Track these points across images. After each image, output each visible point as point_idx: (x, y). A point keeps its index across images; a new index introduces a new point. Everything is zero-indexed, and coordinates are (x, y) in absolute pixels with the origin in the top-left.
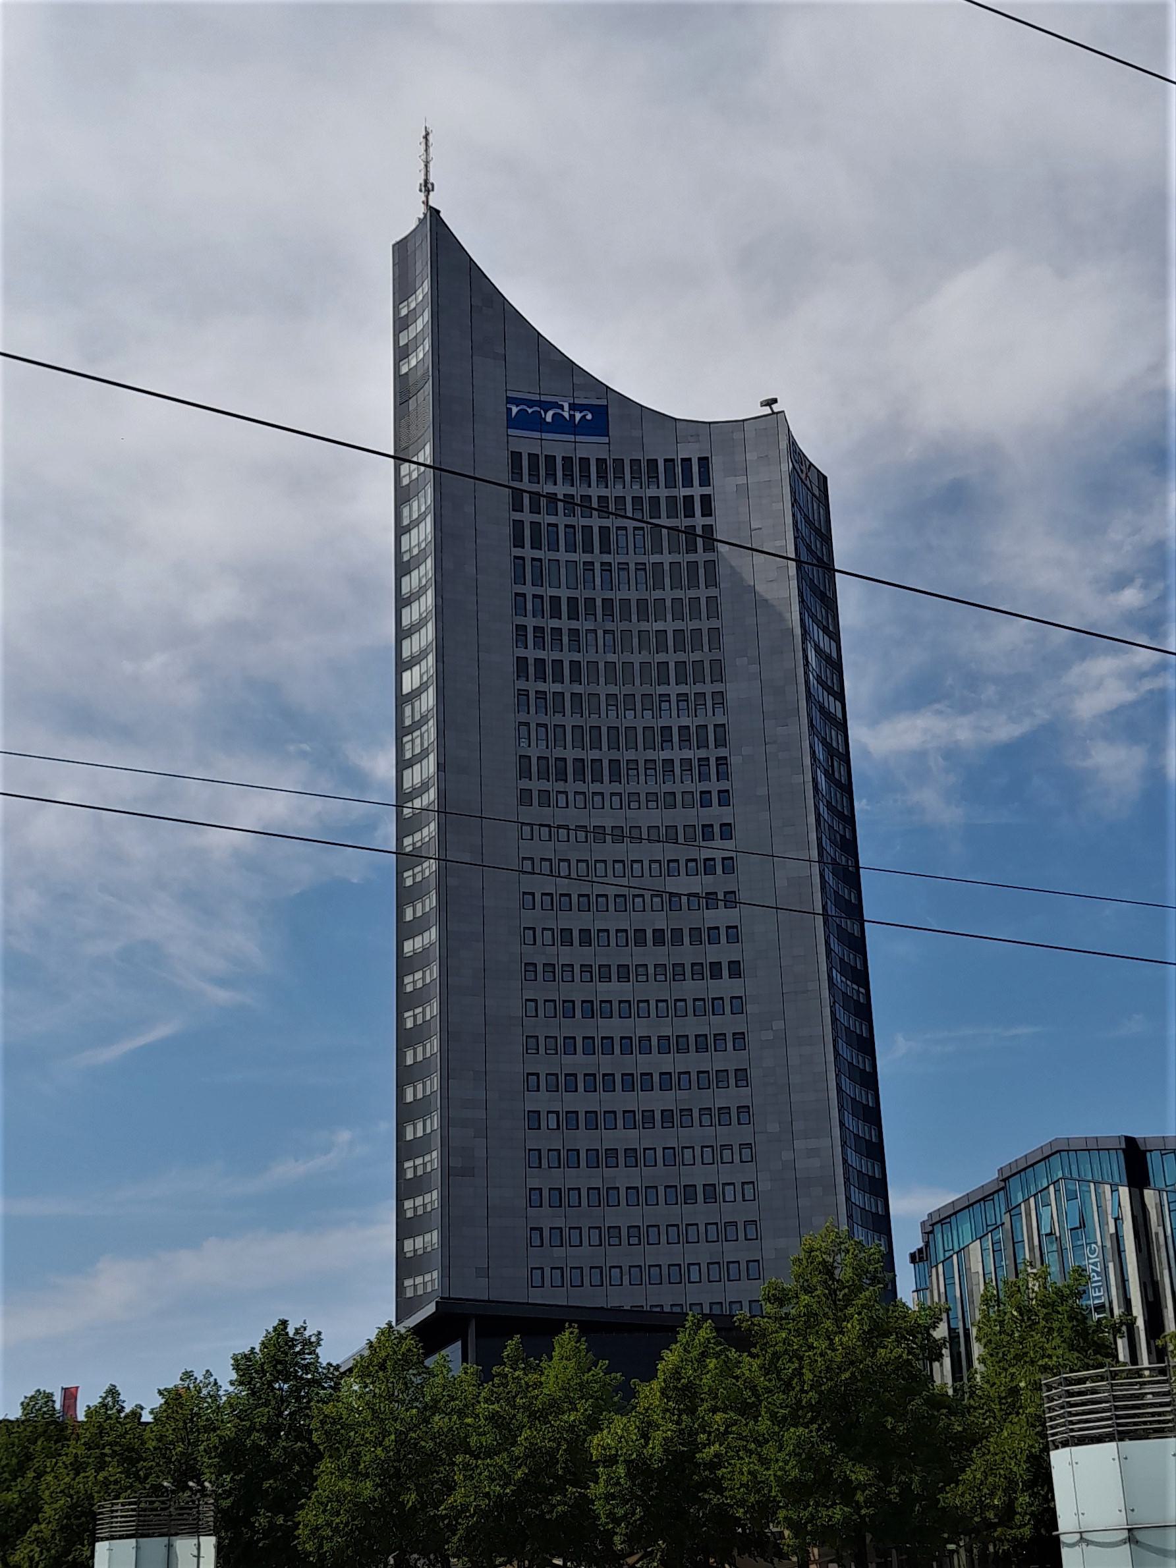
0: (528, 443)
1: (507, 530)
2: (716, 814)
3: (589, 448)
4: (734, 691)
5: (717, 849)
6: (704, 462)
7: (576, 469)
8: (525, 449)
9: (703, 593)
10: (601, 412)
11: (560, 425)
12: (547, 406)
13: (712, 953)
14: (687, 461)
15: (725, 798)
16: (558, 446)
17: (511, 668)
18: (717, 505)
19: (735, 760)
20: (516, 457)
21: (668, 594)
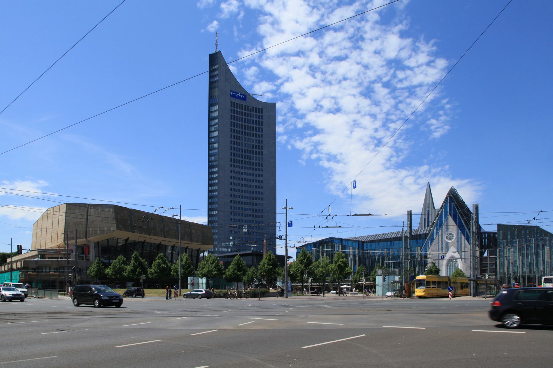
0: (234, 100)
1: (230, 116)
2: (260, 173)
3: (243, 103)
4: (265, 152)
5: (260, 179)
6: (262, 109)
7: (241, 106)
8: (233, 101)
9: (260, 133)
10: (245, 96)
11: (239, 98)
12: (237, 93)
13: (258, 196)
14: (259, 109)
15: (262, 170)
16: (238, 101)
17: (230, 142)
18: (263, 118)
19: (264, 164)
20: (232, 102)
21: (255, 132)
